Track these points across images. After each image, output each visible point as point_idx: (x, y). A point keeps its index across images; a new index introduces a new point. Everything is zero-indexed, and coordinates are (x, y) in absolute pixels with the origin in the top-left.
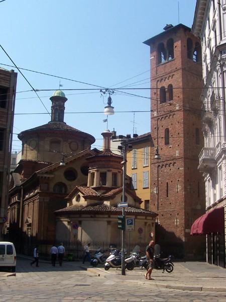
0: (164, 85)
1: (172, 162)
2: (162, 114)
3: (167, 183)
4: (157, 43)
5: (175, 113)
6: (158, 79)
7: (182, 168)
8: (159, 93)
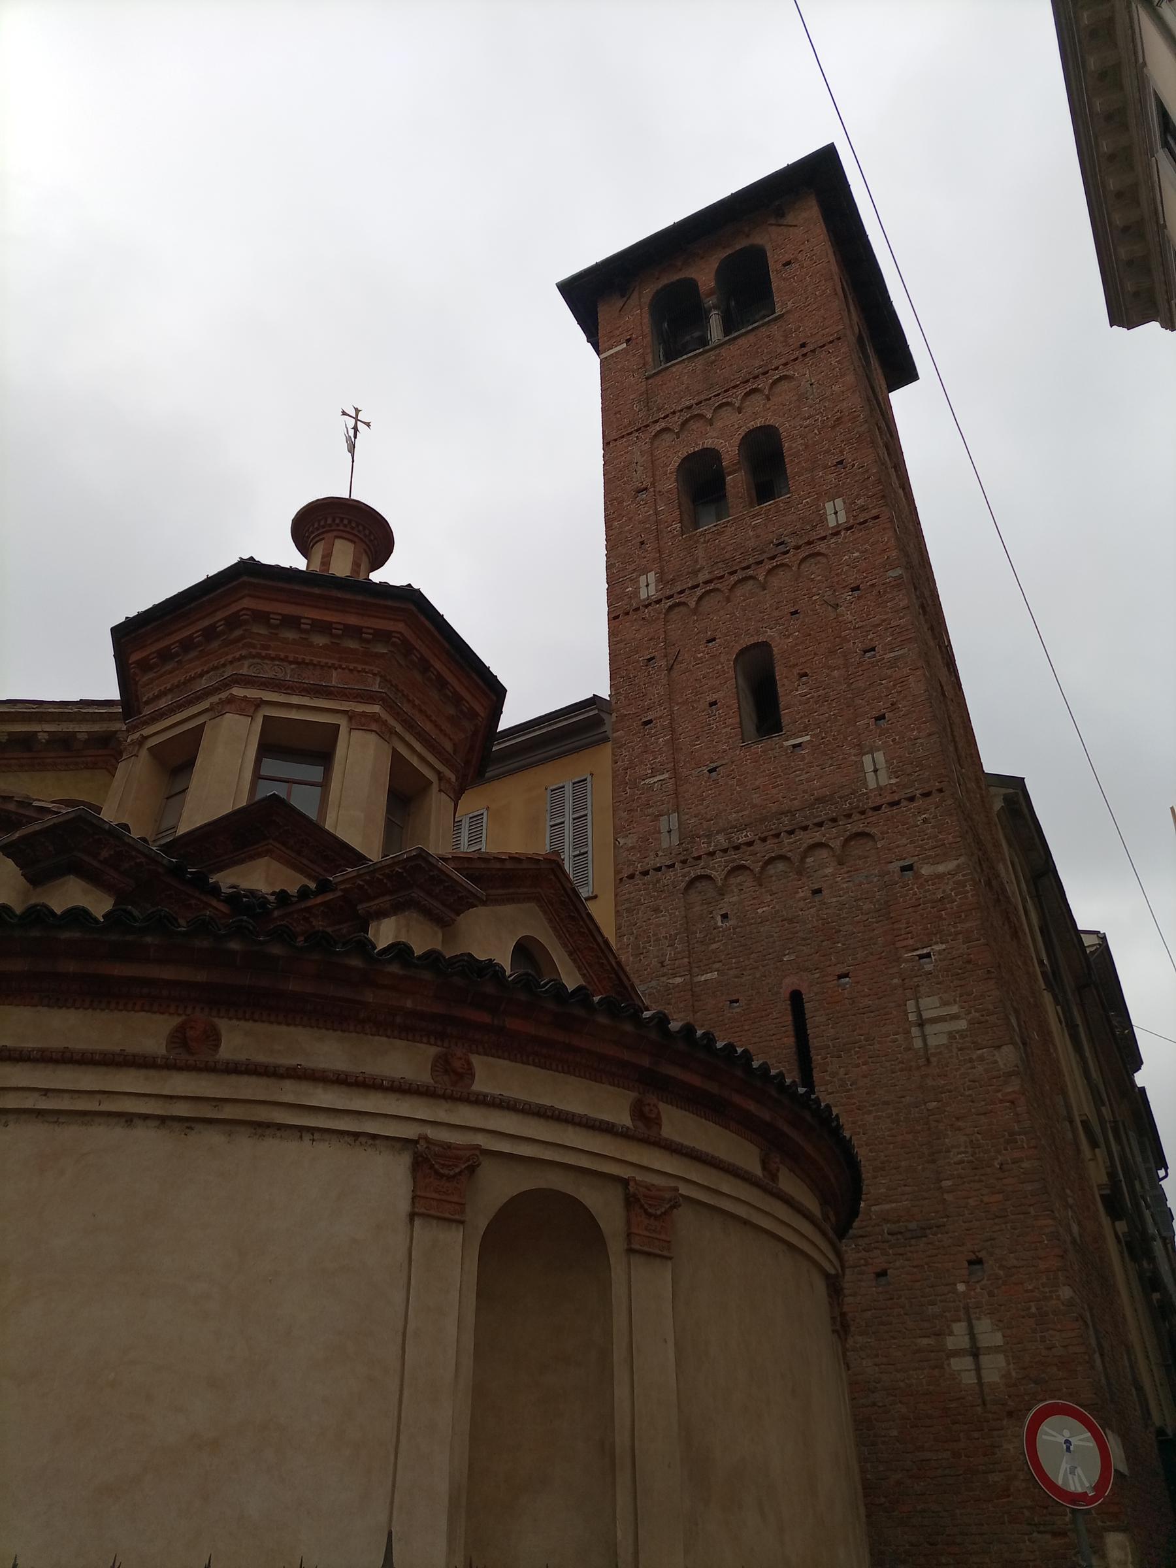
0: (708, 443)
1: (833, 836)
2: (703, 576)
3: (796, 998)
4: (648, 291)
5: (821, 547)
6: (658, 427)
7: (951, 865)
8: (669, 484)
